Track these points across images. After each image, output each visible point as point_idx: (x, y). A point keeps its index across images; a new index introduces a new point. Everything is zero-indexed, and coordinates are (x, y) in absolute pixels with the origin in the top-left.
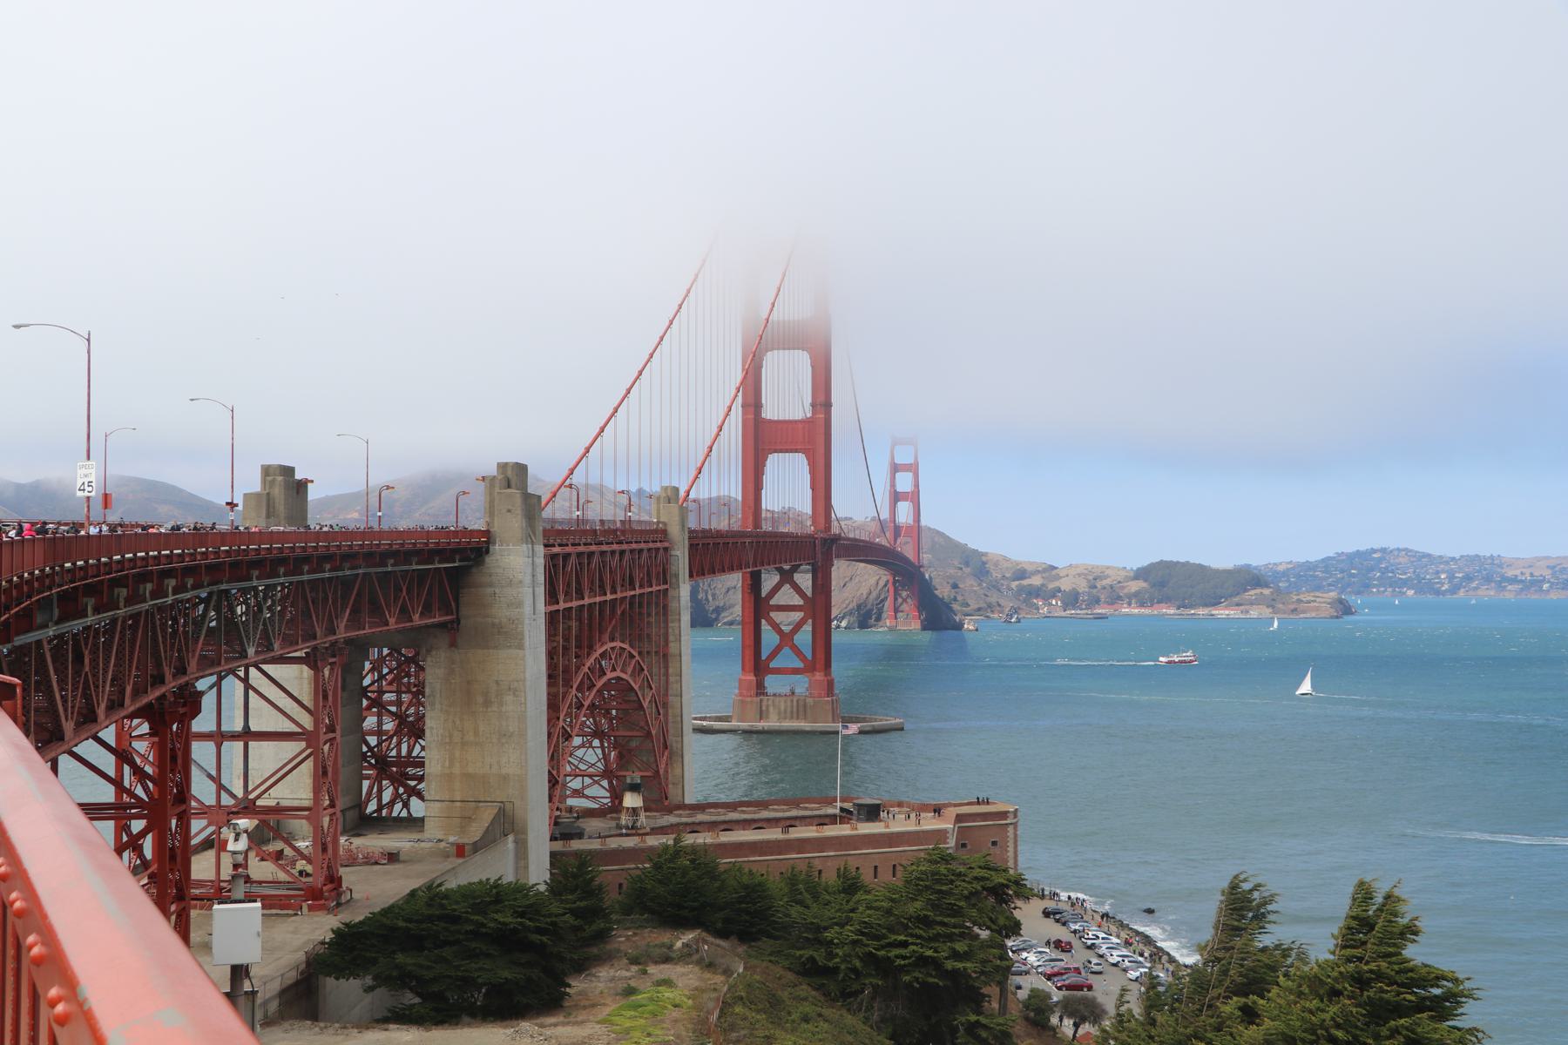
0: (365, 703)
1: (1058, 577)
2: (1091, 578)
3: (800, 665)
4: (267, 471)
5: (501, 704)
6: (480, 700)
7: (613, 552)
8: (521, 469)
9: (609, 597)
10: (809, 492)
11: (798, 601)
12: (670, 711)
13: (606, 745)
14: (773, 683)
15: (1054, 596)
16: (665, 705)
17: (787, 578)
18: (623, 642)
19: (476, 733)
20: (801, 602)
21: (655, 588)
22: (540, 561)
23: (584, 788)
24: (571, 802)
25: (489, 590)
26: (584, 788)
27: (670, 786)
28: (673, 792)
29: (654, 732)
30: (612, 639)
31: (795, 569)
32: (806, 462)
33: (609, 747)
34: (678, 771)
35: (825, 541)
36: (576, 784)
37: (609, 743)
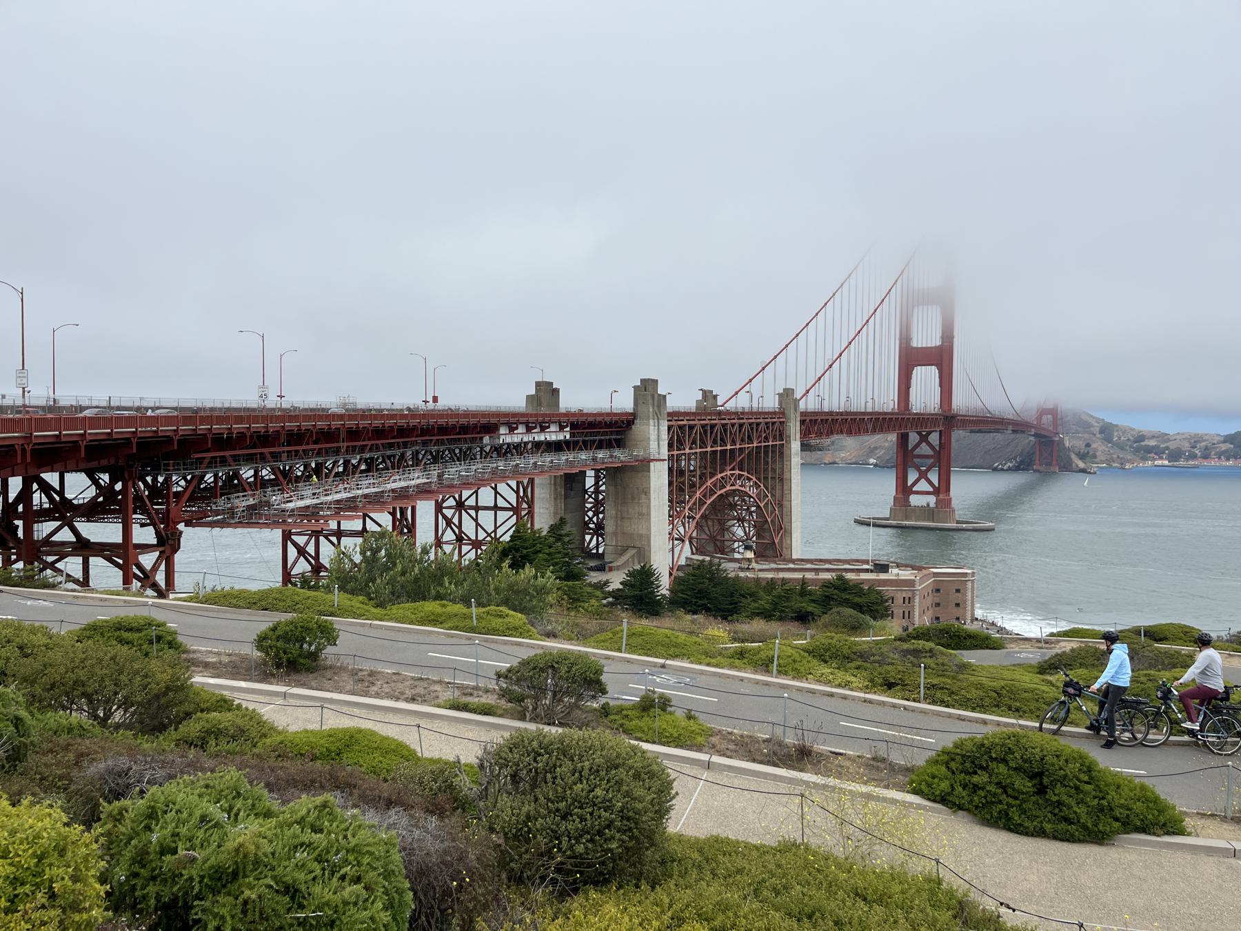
0: (587, 496)
1: (1169, 440)
2: (1193, 441)
3: (931, 489)
4: (538, 384)
5: (639, 500)
6: (630, 496)
7: (733, 425)
8: (656, 382)
9: (729, 447)
10: (938, 389)
11: (931, 453)
12: (784, 509)
13: (746, 525)
14: (915, 500)
15: (1164, 453)
16: (781, 506)
17: (924, 438)
18: (741, 470)
19: (628, 512)
20: (932, 453)
21: (770, 443)
22: (664, 429)
23: (738, 547)
24: (737, 556)
25: (634, 443)
26: (738, 547)
27: (784, 549)
28: (785, 552)
29: (769, 520)
30: (733, 469)
31: (929, 433)
32: (937, 371)
33: (749, 528)
34: (789, 542)
35: (946, 418)
36: (736, 545)
37: (749, 524)
